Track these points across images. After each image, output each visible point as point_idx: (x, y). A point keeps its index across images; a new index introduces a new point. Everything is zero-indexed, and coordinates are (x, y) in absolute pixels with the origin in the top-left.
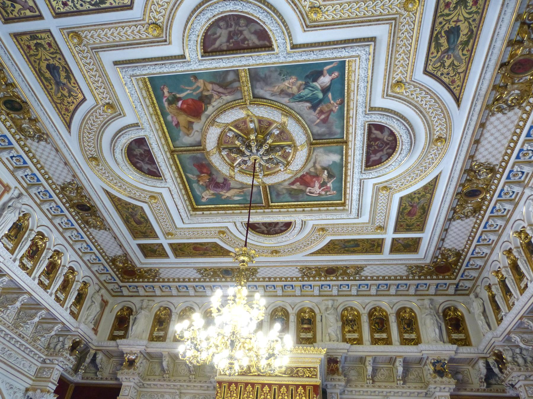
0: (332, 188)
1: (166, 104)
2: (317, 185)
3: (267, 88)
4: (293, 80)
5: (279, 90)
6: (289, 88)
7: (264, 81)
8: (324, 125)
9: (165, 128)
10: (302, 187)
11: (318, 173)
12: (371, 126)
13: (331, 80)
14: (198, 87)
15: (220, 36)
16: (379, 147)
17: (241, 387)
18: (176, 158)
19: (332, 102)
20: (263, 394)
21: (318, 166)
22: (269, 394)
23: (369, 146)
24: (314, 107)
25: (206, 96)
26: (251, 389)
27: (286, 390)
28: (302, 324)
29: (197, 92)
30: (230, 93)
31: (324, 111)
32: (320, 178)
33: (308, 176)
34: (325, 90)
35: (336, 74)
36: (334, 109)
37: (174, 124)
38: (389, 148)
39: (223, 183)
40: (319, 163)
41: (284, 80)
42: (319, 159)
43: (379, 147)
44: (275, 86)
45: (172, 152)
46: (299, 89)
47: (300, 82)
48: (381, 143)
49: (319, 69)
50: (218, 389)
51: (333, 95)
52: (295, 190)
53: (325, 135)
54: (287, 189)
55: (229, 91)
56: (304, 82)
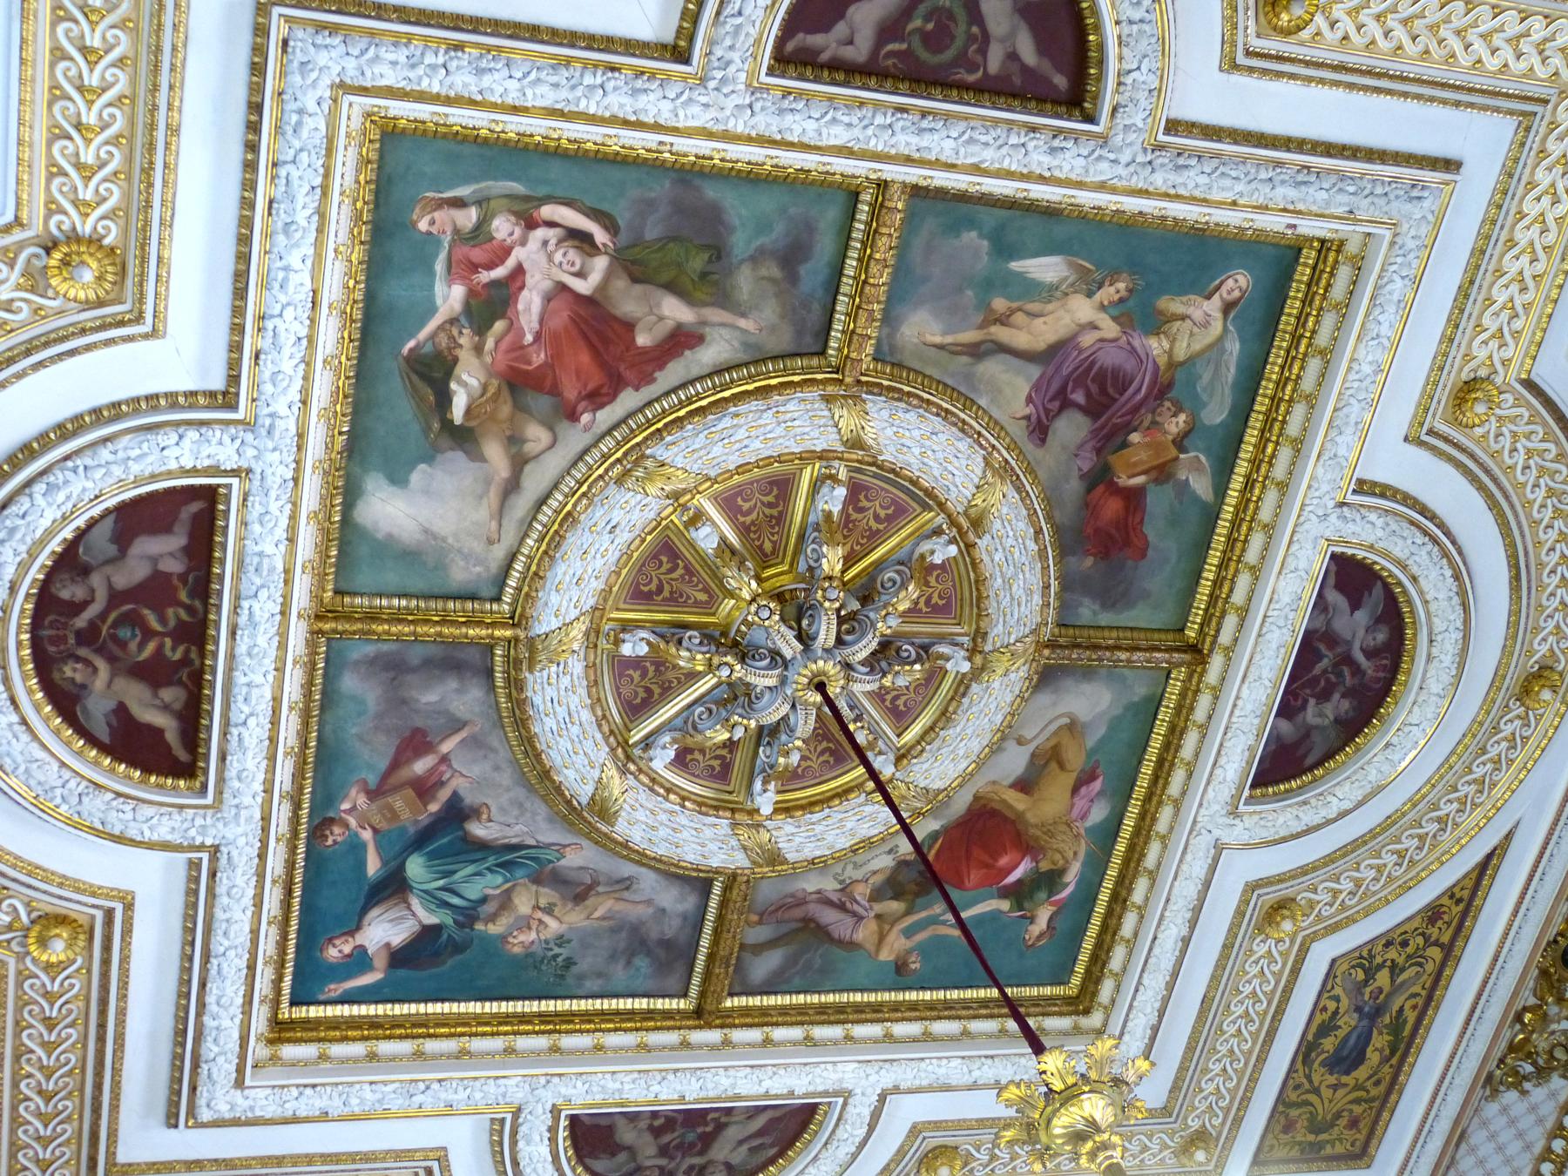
0: (439, 266)
1: (1072, 876)
2: (530, 304)
3: (642, 912)
4: (522, 938)
5: (590, 902)
6: (549, 910)
7: (643, 942)
8: (419, 722)
9: (1143, 782)
10: (629, 302)
11: (506, 409)
12: (182, 755)
13: (358, 928)
14: (908, 933)
15: (741, 1142)
16: (133, 620)
18: (1197, 616)
19: (367, 835)
21: (495, 453)
23: (197, 633)
24: (457, 813)
25: (896, 897)
29: (923, 914)
30: (801, 901)
31: (410, 792)
32: (502, 362)
33: (571, 392)
34: (392, 887)
35: (334, 953)
36: (362, 800)
37: (1097, 785)
38: (77, 608)
39: (1066, 404)
40: (488, 482)
41: (561, 940)
42: (482, 513)
43: (133, 620)
44: (603, 918)
45: (1197, 653)
46: (506, 902)
47: (494, 929)
48: (123, 645)
49: (402, 973)
51: (361, 864)
52: (672, 287)
53: (428, 664)
54: (724, 299)
55: (798, 913)
56: (479, 926)
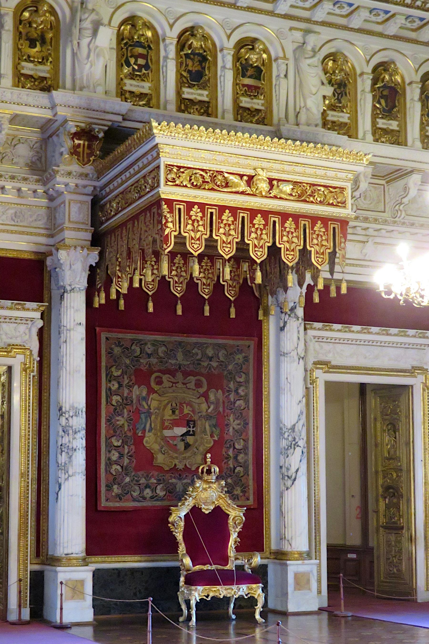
17: (212, 213)
20: (253, 230)
22: (264, 232)
26: (231, 219)
27: (294, 226)
28: (244, 76)
50: (168, 215)
